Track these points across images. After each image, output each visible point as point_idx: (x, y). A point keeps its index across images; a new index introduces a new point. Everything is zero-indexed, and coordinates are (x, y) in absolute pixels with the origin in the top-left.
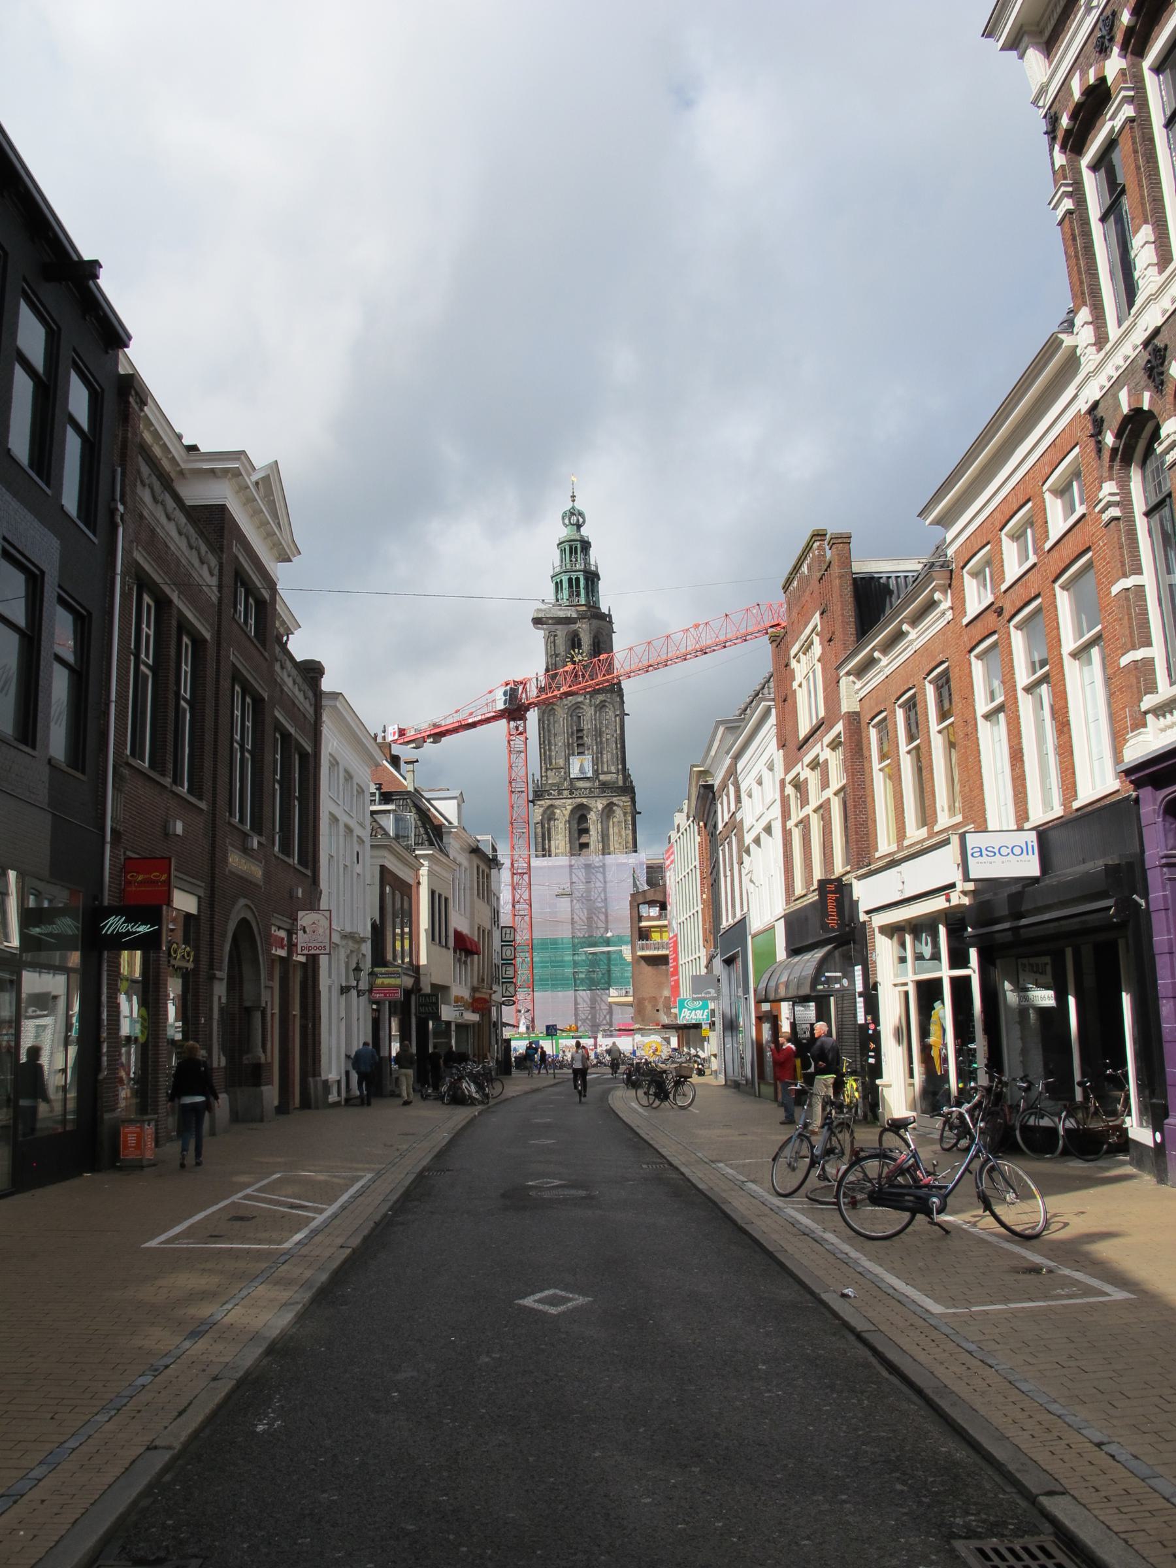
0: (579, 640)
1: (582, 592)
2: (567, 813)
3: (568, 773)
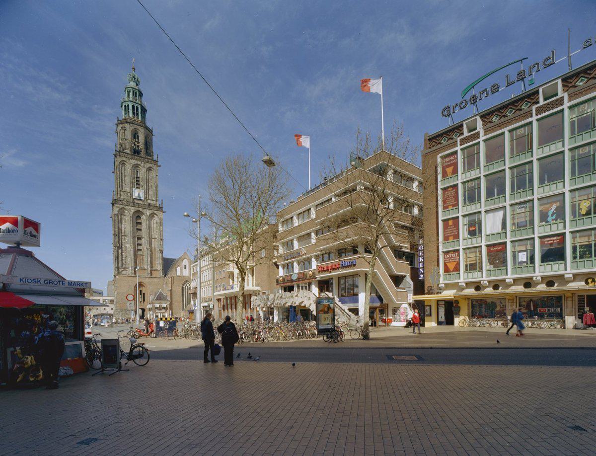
0: (138, 136)
1: (140, 115)
2: (131, 213)
3: (131, 195)
